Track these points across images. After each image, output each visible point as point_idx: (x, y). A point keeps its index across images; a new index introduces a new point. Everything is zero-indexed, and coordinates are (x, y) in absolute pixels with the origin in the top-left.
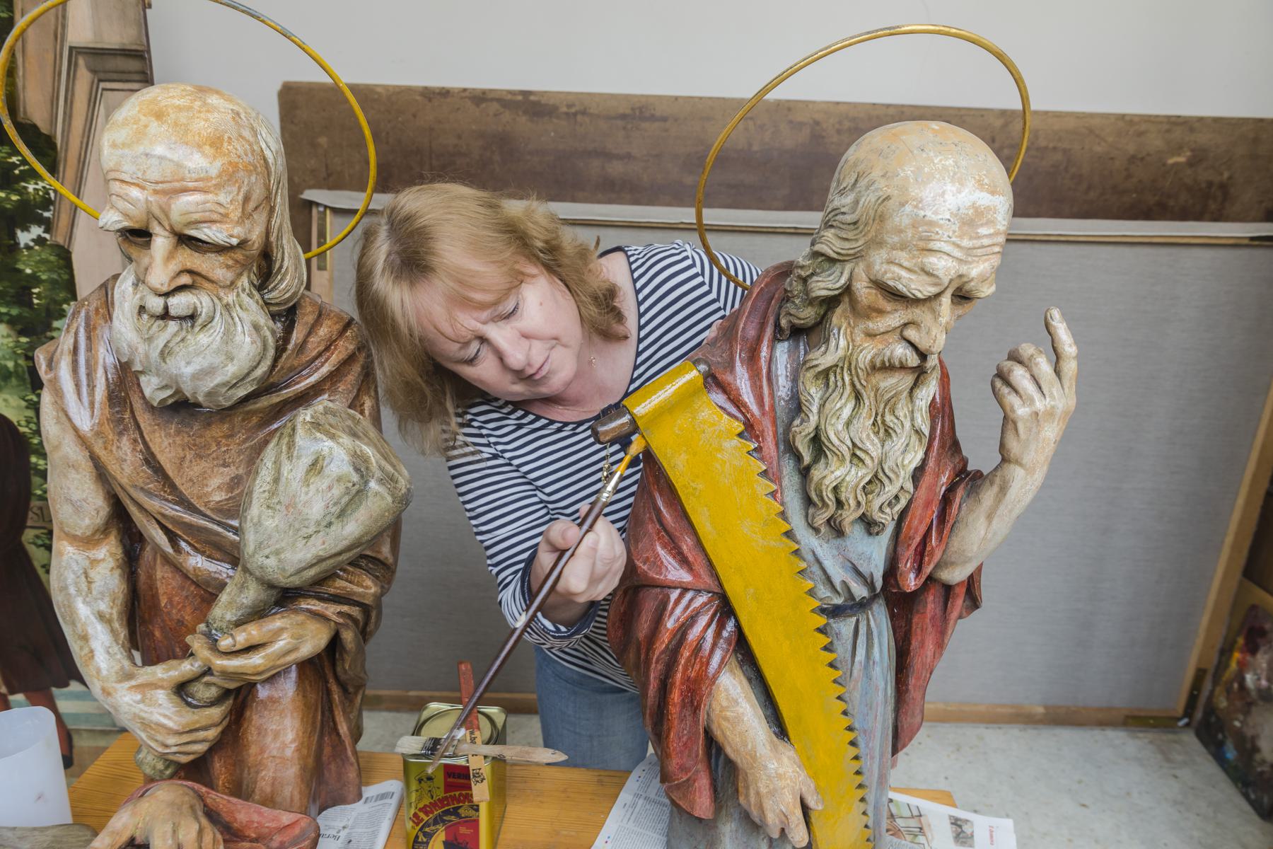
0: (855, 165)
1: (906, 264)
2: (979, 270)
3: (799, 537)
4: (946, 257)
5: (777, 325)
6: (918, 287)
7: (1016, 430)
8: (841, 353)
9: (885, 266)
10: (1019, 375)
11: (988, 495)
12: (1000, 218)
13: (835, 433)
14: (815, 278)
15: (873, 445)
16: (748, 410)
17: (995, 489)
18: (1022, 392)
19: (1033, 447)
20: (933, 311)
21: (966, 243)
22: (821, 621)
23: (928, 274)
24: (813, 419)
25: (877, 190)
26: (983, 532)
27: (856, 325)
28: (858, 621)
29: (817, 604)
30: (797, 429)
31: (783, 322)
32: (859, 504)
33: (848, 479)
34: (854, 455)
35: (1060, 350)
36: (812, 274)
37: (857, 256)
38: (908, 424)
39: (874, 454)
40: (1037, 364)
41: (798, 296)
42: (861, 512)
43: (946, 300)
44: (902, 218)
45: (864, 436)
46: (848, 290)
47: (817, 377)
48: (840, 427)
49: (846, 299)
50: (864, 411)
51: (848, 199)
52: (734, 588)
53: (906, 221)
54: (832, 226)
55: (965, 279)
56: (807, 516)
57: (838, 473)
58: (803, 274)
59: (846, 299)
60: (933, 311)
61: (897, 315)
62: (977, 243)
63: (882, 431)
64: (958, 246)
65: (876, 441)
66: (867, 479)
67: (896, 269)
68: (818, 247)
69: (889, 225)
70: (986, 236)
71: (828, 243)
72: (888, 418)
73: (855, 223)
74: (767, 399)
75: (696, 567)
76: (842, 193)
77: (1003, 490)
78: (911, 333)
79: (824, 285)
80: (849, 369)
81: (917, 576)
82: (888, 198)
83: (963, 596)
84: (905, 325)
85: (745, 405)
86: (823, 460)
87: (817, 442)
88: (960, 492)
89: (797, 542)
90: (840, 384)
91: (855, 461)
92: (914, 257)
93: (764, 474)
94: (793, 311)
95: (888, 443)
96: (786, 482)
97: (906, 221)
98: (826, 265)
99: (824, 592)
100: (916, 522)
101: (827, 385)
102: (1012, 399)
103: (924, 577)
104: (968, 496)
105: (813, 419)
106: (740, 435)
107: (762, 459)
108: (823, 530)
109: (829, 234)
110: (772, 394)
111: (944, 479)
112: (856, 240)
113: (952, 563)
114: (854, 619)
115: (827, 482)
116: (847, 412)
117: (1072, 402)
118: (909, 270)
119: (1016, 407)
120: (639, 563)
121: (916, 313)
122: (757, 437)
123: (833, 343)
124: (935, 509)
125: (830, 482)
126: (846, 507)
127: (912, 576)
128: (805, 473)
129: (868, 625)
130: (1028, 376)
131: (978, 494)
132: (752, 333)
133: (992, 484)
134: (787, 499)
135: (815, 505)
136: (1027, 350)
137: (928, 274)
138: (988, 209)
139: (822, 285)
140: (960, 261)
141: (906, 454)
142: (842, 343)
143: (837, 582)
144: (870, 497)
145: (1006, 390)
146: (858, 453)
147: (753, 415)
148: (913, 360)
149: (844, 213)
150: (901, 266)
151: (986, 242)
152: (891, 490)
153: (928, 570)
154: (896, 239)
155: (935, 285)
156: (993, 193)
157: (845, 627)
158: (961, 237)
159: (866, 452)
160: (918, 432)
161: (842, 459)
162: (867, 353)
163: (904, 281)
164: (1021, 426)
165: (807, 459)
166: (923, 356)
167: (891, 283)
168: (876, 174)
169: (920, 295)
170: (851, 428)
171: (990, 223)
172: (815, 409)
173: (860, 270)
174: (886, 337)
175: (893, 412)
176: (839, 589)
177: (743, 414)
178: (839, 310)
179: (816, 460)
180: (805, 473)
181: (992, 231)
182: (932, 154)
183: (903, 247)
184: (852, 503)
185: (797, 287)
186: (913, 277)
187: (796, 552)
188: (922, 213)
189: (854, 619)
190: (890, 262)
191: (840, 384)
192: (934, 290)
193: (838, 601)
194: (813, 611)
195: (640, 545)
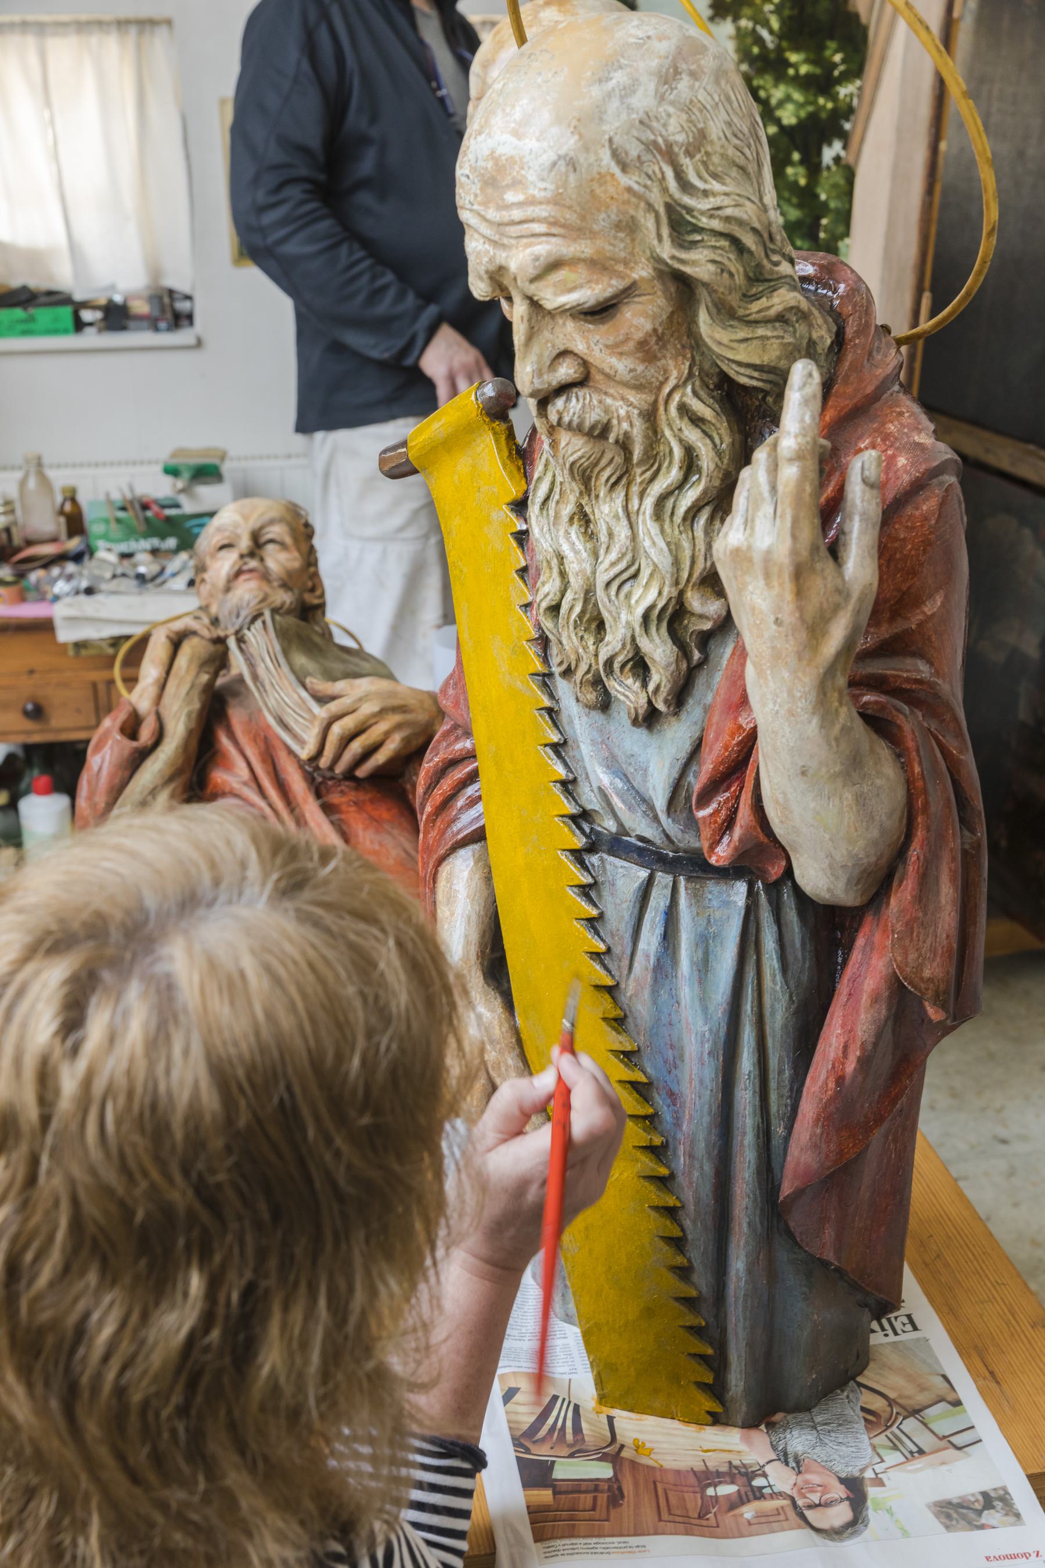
4: (476, 236)
12: (531, 176)
15: (577, 552)
21: (492, 214)
28: (650, 882)
29: (572, 809)
38: (622, 532)
45: (561, 533)
57: (546, 589)
62: (505, 216)
64: (484, 219)
65: (579, 546)
66: (578, 609)
70: (514, 205)
72: (596, 511)
103: (732, 846)
114: (643, 874)
138: (511, 160)
140: (494, 243)
143: (595, 786)
151: (517, 214)
152: (614, 640)
158: (485, 204)
181: (521, 197)
189: (643, 874)
193: (609, 825)
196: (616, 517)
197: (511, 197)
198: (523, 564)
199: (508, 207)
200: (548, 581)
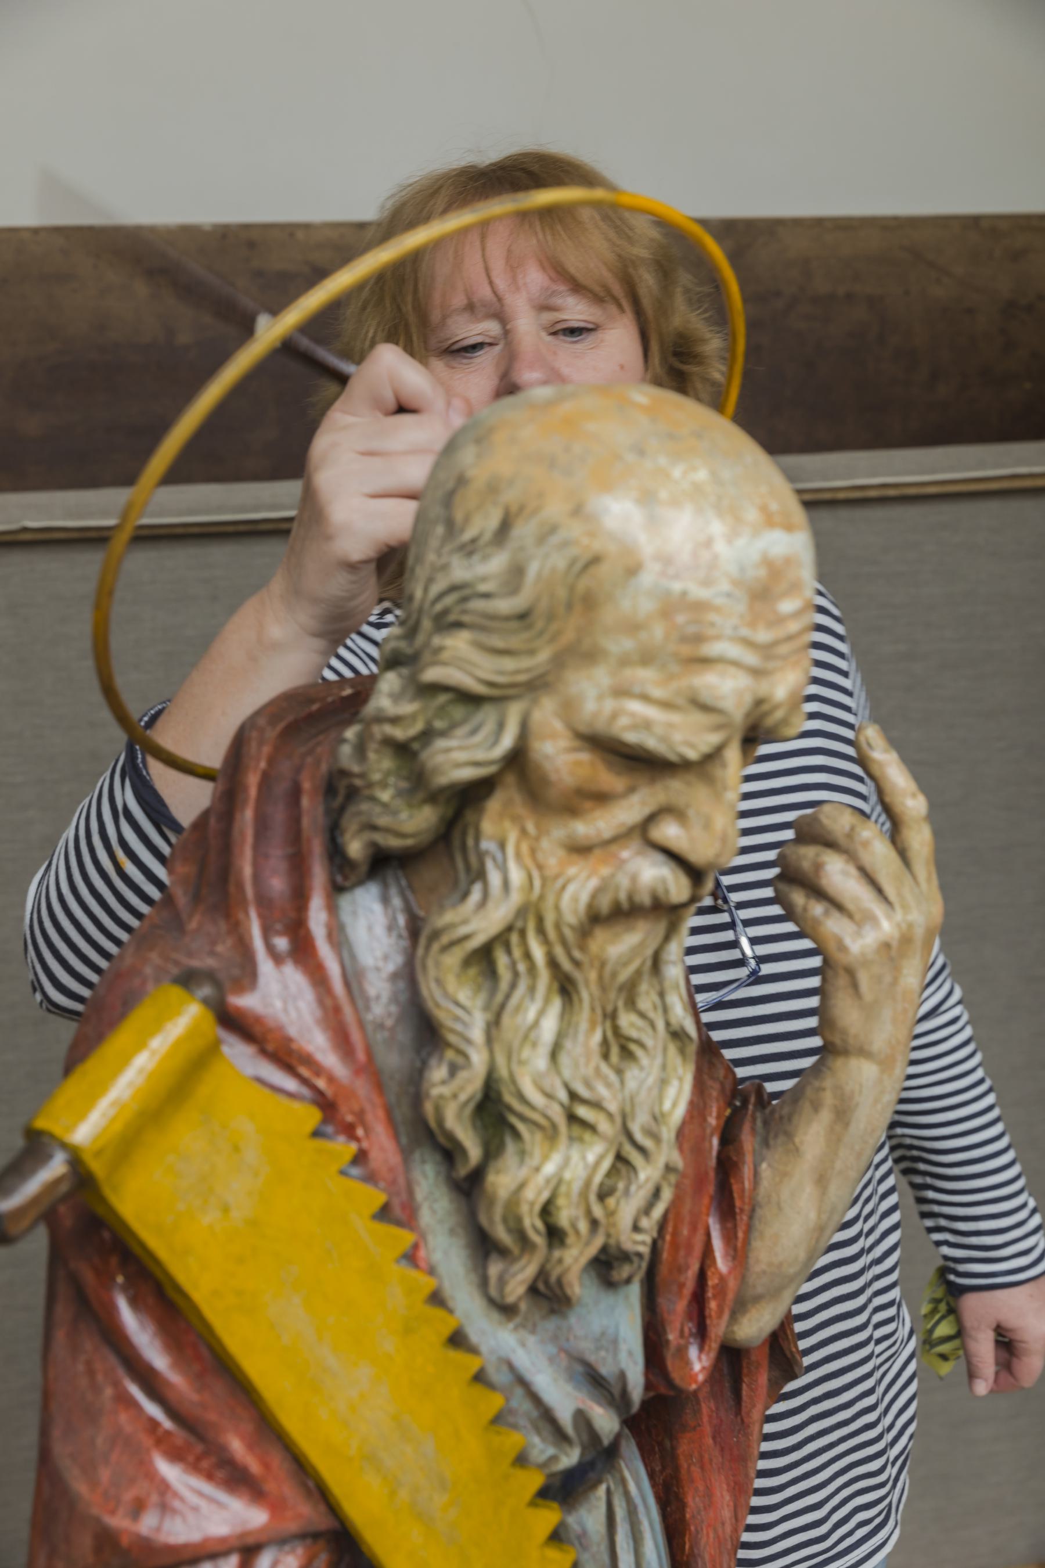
0: (493, 489)
1: (657, 693)
2: (785, 684)
3: (474, 1337)
4: (732, 670)
5: (336, 853)
6: (684, 736)
7: (855, 985)
8: (516, 898)
9: (609, 705)
10: (837, 874)
11: (812, 1135)
13: (533, 1079)
14: (441, 743)
16: (318, 1069)
17: (826, 1116)
18: (850, 906)
19: (887, 1014)
20: (710, 780)
21: (763, 636)
22: (549, 1517)
23: (705, 708)
24: (478, 1059)
25: (565, 544)
26: (813, 1215)
27: (541, 832)
28: (609, 1492)
29: (536, 1481)
30: (446, 1090)
31: (355, 848)
32: (594, 1223)
33: (567, 1175)
34: (572, 1118)
35: (898, 809)
36: (427, 735)
37: (535, 686)
38: (661, 1025)
39: (613, 1107)
40: (866, 844)
41: (384, 785)
42: (599, 1242)
43: (733, 754)
44: (637, 600)
46: (518, 760)
47: (468, 962)
48: (541, 1062)
49: (510, 779)
50: (583, 1017)
51: (496, 563)
52: (365, 1505)
53: (646, 606)
54: (458, 625)
55: (765, 707)
56: (484, 1283)
57: (550, 1168)
58: (399, 733)
59: (510, 779)
60: (710, 780)
61: (635, 799)
63: (615, 1051)
65: (613, 1077)
67: (636, 707)
68: (432, 674)
69: (608, 615)
71: (458, 662)
72: (627, 1021)
73: (523, 616)
74: (356, 1036)
75: (270, 1487)
76: (469, 549)
77: (843, 1115)
78: (669, 832)
79: (463, 754)
80: (541, 930)
81: (701, 1349)
82: (595, 560)
83: (765, 1363)
84: (651, 819)
85: (308, 1060)
86: (511, 1147)
87: (493, 1111)
88: (748, 1141)
89: (473, 1350)
90: (522, 967)
91: (577, 1130)
92: (671, 677)
93: (384, 1214)
94: (383, 821)
95: (632, 1075)
96: (426, 1217)
97: (646, 606)
98: (458, 712)
99: (541, 1448)
100: (685, 1232)
101: (492, 973)
102: (834, 926)
104: (766, 1143)
105: (478, 1059)
106: (316, 1134)
107: (371, 1178)
108: (523, 1306)
109: (458, 643)
110: (361, 1024)
111: (712, 1121)
112: (532, 652)
113: (757, 1299)
115: (529, 1194)
116: (549, 1026)
117: (936, 909)
118: (666, 705)
119: (848, 941)
120: (118, 1521)
121: (673, 790)
122: (349, 1131)
123: (494, 878)
124: (711, 1188)
125: (534, 1195)
126: (571, 1239)
127: (693, 1352)
128: (469, 1187)
129: (627, 1494)
130: (853, 871)
131: (789, 1136)
132: (278, 884)
133: (816, 1107)
134: (437, 1257)
135: (503, 1252)
136: (838, 820)
137: (705, 708)
139: (461, 756)
140: (757, 673)
141: (664, 1088)
142: (516, 876)
143: (565, 1415)
144: (611, 1201)
145: (817, 909)
146: (582, 1111)
147: (331, 1079)
148: (678, 888)
149: (486, 596)
150: (645, 698)
152: (647, 1174)
153: (718, 1329)
154: (627, 644)
155: (718, 728)
156: (789, 528)
157: (590, 1517)
159: (596, 1105)
160: (677, 1035)
161: (551, 1134)
162: (578, 889)
163: (659, 730)
164: (864, 979)
165: (474, 1152)
166: (695, 873)
167: (631, 737)
168: (555, 509)
169: (692, 755)
170: (564, 1059)
171: (795, 587)
172: (477, 1034)
173: (546, 713)
174: (614, 848)
175: (631, 1003)
176: (569, 1428)
177: (304, 1081)
178: (494, 805)
179: (492, 1152)
180: (469, 1187)
182: (663, 461)
183: (646, 658)
184: (583, 1226)
185: (381, 764)
186: (675, 718)
187: (480, 1378)
188: (677, 587)
190: (621, 692)
191: (522, 967)
192: (714, 739)
193: (570, 1458)
194: (532, 1504)
195: (105, 1475)
196: (655, 1007)
197: (787, 606)
198: (381, 1198)
199: (780, 620)
200: (545, 1158)
